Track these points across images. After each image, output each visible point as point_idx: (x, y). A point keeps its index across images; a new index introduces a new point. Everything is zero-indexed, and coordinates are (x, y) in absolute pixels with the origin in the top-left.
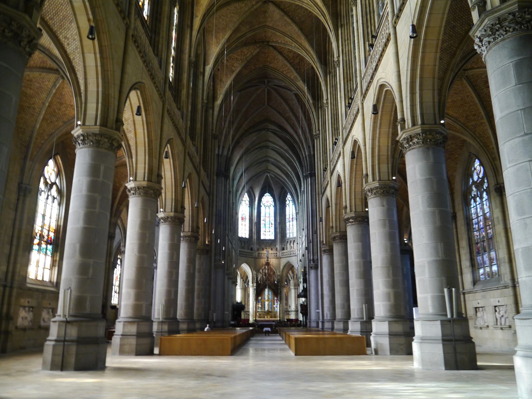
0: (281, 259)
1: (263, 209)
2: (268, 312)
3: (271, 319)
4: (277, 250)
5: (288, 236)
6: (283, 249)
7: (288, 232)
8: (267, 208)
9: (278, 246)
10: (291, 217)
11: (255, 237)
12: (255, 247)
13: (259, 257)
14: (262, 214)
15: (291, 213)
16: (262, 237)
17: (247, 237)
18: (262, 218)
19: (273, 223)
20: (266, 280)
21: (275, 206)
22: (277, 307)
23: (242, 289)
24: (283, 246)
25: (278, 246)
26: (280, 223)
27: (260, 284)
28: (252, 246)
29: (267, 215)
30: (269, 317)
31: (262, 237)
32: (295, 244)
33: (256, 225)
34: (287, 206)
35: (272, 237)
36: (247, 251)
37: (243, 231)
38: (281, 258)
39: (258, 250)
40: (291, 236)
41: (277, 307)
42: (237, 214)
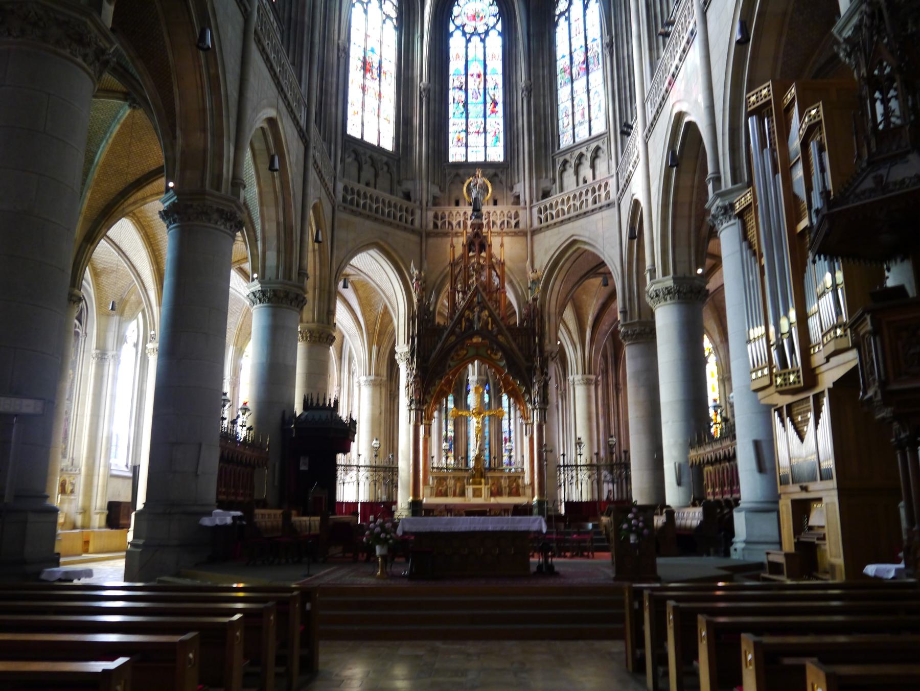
0: (538, 238)
1: (456, 43)
2: (480, 473)
3: (493, 500)
4: (517, 200)
5: (565, 141)
6: (546, 194)
7: (564, 121)
8: (476, 40)
9: (523, 188)
10: (579, 57)
11: (421, 147)
12: (424, 189)
13: (440, 230)
14: (455, 66)
15: (578, 42)
16: (455, 154)
17: (388, 144)
18: (455, 79)
19: (499, 96)
20: (469, 306)
21: (508, 35)
22: (520, 453)
24: (545, 184)
26: (529, 90)
27: (439, 330)
28: (408, 185)
29: (475, 68)
30: (485, 489)
31: (455, 154)
32: (601, 165)
33: (425, 98)
34: (562, 23)
35: (497, 154)
36: (387, 196)
37: (372, 115)
38: (534, 232)
39: (436, 202)
40: (582, 134)
41: (520, 453)
42: (344, 53)
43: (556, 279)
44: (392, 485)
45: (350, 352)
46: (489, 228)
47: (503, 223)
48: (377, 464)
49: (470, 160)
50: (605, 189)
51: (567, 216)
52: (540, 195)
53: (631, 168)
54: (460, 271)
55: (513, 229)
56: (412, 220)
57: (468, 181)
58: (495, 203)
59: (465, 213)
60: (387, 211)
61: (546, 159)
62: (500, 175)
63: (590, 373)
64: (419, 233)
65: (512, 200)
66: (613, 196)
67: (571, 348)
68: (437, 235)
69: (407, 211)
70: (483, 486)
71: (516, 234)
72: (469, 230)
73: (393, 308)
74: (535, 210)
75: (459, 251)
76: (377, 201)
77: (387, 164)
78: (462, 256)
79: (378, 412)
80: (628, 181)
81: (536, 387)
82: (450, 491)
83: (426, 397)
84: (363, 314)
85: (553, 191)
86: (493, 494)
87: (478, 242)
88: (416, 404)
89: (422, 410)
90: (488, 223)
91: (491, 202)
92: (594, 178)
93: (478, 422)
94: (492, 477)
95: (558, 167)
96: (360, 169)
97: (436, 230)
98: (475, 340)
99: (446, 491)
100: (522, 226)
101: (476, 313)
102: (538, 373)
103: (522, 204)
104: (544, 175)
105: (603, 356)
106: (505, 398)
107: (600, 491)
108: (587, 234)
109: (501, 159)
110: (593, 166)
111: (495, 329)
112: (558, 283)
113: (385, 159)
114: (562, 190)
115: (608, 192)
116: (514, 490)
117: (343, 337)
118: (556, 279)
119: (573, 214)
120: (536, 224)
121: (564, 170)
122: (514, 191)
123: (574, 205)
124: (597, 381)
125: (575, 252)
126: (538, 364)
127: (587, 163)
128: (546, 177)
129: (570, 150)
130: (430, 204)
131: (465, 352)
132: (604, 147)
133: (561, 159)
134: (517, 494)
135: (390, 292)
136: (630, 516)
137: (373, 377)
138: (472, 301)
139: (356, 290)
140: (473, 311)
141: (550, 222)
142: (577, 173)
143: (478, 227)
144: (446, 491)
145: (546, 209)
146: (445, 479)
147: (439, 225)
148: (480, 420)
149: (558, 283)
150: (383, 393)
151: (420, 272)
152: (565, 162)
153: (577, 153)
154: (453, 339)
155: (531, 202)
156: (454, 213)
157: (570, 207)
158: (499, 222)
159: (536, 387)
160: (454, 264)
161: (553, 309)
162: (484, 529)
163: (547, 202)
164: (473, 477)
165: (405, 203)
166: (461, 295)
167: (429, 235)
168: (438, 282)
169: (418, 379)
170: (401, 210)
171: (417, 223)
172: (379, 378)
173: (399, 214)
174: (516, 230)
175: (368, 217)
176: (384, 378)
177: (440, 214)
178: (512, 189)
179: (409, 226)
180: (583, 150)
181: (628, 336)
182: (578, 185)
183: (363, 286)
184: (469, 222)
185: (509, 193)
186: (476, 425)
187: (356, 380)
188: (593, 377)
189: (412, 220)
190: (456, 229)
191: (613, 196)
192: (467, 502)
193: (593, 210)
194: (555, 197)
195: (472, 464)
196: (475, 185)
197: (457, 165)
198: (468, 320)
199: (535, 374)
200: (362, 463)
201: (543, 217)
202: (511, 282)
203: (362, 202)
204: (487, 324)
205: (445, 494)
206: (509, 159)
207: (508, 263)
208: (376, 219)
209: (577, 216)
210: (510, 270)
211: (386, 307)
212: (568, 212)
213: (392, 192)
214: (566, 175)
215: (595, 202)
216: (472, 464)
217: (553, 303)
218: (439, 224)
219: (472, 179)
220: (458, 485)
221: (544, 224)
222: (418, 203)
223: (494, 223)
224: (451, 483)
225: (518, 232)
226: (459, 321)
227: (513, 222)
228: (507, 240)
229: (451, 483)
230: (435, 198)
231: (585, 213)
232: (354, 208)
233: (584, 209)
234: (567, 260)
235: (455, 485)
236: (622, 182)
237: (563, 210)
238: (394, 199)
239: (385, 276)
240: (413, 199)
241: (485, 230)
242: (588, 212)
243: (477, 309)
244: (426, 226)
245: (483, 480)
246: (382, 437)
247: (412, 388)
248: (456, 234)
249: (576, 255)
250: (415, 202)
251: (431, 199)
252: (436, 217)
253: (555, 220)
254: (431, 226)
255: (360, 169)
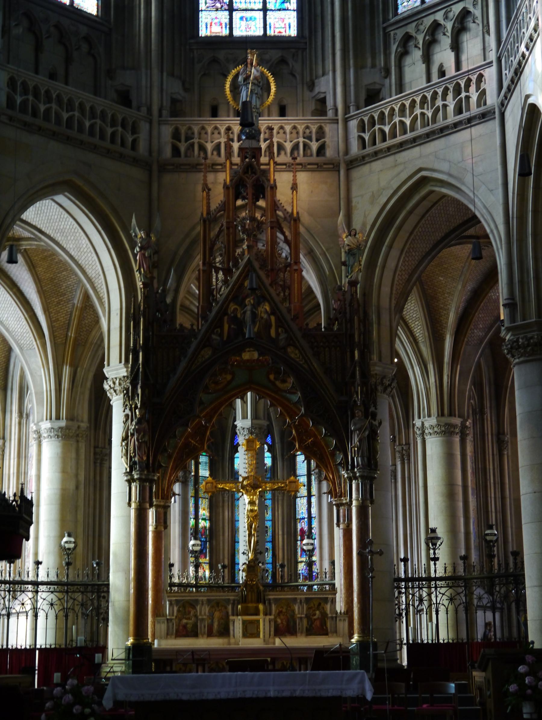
0: (361, 174)
3: (278, 642)
4: (321, 107)
6: (373, 96)
9: (332, 85)
12: (154, 85)
20: (237, 295)
22: (329, 554)
23: (66, 436)
24: (371, 77)
25: (332, 85)
30: (264, 622)
32: (472, 46)
38: (353, 164)
39: (176, 109)
41: (329, 554)
43: (390, 247)
44: (101, 616)
45: (23, 377)
46: (271, 156)
47: (296, 147)
48: (71, 578)
49: (237, 33)
50: (478, 88)
51: (409, 135)
52: (363, 96)
53: (523, 48)
54: (220, 231)
55: (314, 159)
56: (134, 142)
57: (234, 72)
58: (282, 112)
59: (229, 129)
60: (87, 124)
61: (372, 35)
62: (291, 62)
63: (451, 414)
64: (144, 164)
65: (312, 106)
66: (492, 99)
67: (417, 369)
68: (179, 168)
69: (123, 126)
70: (261, 618)
71: (318, 168)
72: (236, 159)
73: (100, 299)
74: (353, 124)
75: (218, 195)
76: (70, 106)
77: (87, 39)
78: (224, 206)
79: (72, 486)
80: (518, 72)
81: (356, 440)
82: (203, 627)
83: (160, 457)
84: (46, 310)
85: (385, 92)
86: (279, 632)
87: (252, 181)
88: (141, 471)
89: (151, 481)
90: (270, 147)
91: (275, 110)
92: (458, 67)
93: (252, 503)
94: (276, 600)
95: (394, 47)
96: (38, 48)
97: (176, 160)
98: (246, 356)
99: (195, 626)
100: (329, 153)
101: (249, 308)
102: (358, 413)
103: (330, 113)
104: (369, 61)
105: (474, 383)
106: (300, 458)
107: (471, 624)
108: (444, 166)
109: (293, 32)
110: (456, 47)
111: (283, 336)
112: (395, 253)
113: (84, 30)
114: (400, 88)
115: (484, 92)
116: (318, 623)
117: (10, 350)
118: (390, 247)
119: (420, 131)
120: (355, 148)
121: (404, 53)
122: (317, 90)
123: (423, 114)
124: (464, 427)
125: (424, 198)
126: (358, 398)
127: (446, 41)
128: (373, 66)
129: (415, 16)
130: (164, 113)
131: (229, 377)
132: (477, 12)
133: (400, 33)
134: (323, 632)
135: (93, 270)
136: (522, 669)
137: (63, 423)
138: (242, 284)
139: (32, 267)
140: (242, 305)
141: (380, 145)
142: (427, 59)
143: (251, 153)
144: (195, 626)
145: (372, 123)
146: (193, 604)
147: (183, 149)
148: (256, 498)
149: (395, 253)
150: (82, 451)
151: (148, 235)
152: (408, 38)
153: (428, 21)
154: (207, 353)
155: (346, 109)
156: (209, 130)
157: (416, 118)
158: (288, 146)
159: (356, 440)
160: (208, 221)
161: (385, 302)
162: (262, 695)
163: (375, 110)
164: (244, 600)
165: (121, 112)
166: (221, 275)
167: (163, 168)
168: (181, 251)
169: (145, 425)
170: (113, 124)
171: (142, 146)
172: (75, 424)
173: (109, 131)
174: (320, 159)
175: (54, 135)
176: (84, 425)
177: (183, 130)
178: (312, 86)
179: (128, 151)
180: (439, 16)
181: (519, 347)
182: (429, 80)
183: (45, 259)
184: (236, 146)
185: (307, 93)
186: (248, 507)
187: (33, 427)
188: (457, 421)
189: (134, 142)
190: (212, 157)
191: (492, 99)
192: (233, 646)
193: (456, 125)
194: (390, 102)
195: (241, 576)
196: (247, 79)
197: (215, 42)
198: (234, 320)
199: (353, 416)
200: (42, 577)
201: (366, 136)
202: (311, 254)
203: (42, 108)
204: (268, 326)
205: (194, 633)
206: (306, 33)
207: (305, 218)
208: (68, 140)
209: (428, 135)
210: (308, 230)
211: (87, 297)
212: (412, 129)
213: (96, 93)
214: (408, 60)
215: (459, 110)
216: (241, 576)
217: (386, 289)
218: (183, 147)
219: (240, 67)
220: (217, 614)
221: (369, 150)
222: (144, 109)
223: (281, 147)
224: (204, 611)
225: (323, 164)
226: (218, 322)
227: (314, 146)
228: (302, 177)
229: (204, 611)
230: (174, 101)
231: (442, 130)
232: (29, 118)
233: (441, 123)
234: (410, 212)
235: (211, 616)
236: (508, 74)
237: (402, 123)
238: (101, 103)
239: (85, 241)
240: (134, 104)
241: (264, 159)
242: (447, 127)
243: (249, 301)
244: (160, 152)
245: (261, 607)
246: (80, 530)
247: (134, 441)
248: (214, 168)
249: (426, 204)
250: (139, 109)
251: (167, 103)
252: (176, 135)
253: (390, 142)
254: (168, 152)
255: (38, 48)
